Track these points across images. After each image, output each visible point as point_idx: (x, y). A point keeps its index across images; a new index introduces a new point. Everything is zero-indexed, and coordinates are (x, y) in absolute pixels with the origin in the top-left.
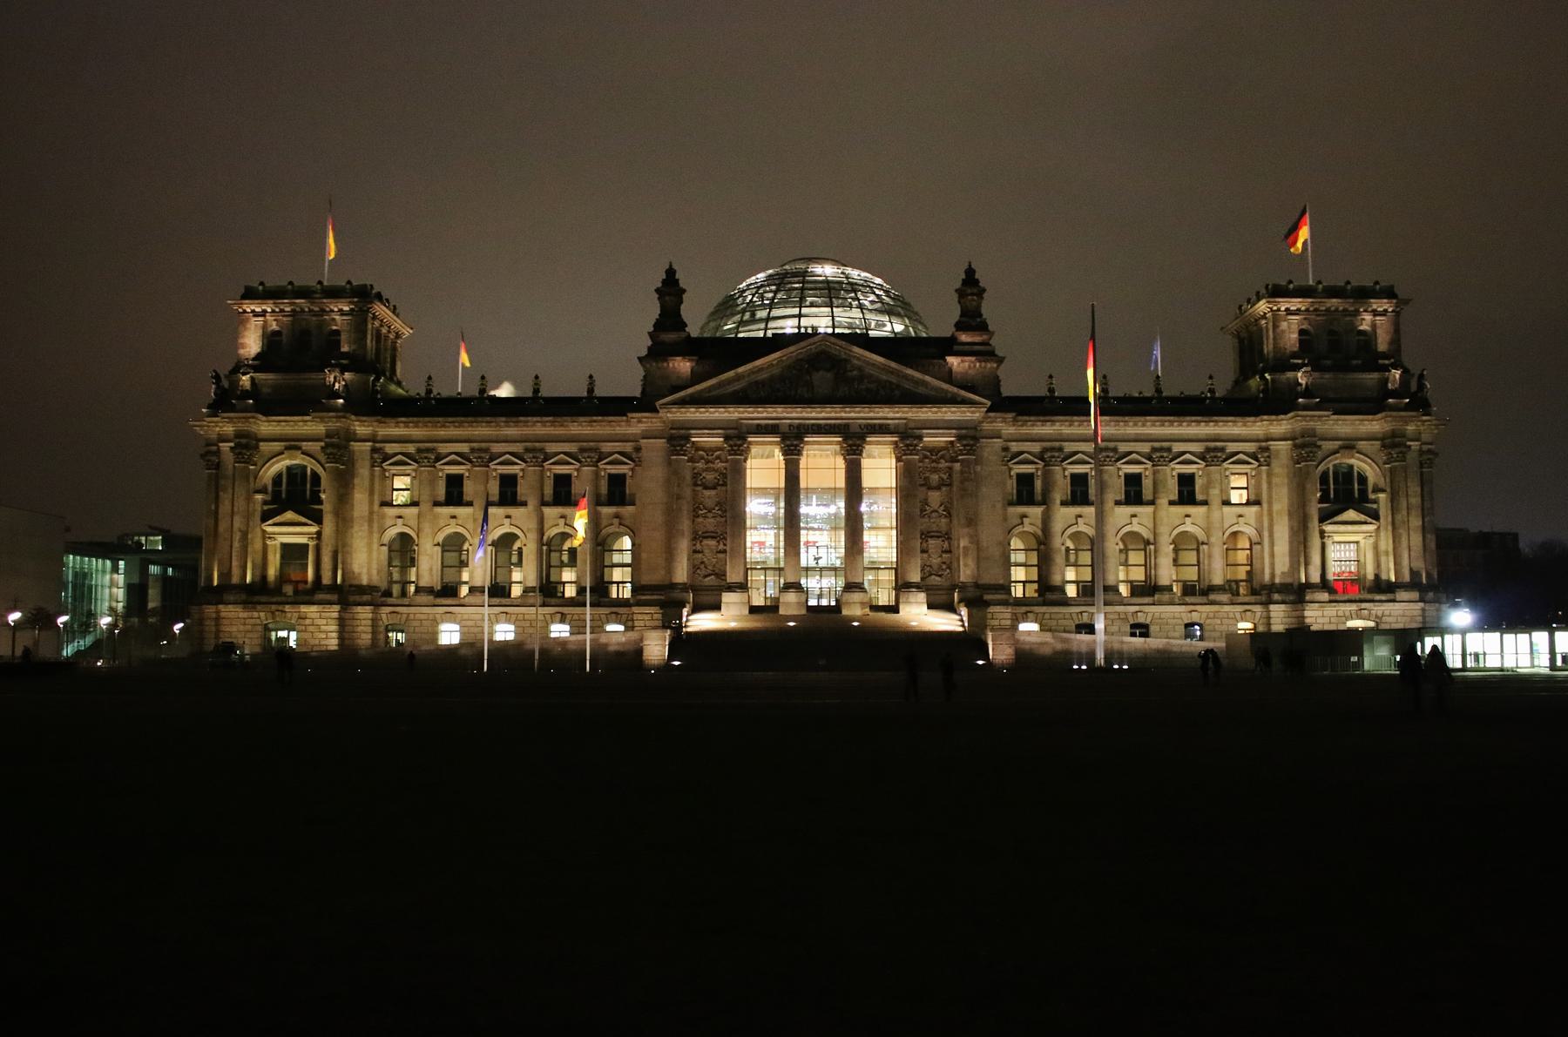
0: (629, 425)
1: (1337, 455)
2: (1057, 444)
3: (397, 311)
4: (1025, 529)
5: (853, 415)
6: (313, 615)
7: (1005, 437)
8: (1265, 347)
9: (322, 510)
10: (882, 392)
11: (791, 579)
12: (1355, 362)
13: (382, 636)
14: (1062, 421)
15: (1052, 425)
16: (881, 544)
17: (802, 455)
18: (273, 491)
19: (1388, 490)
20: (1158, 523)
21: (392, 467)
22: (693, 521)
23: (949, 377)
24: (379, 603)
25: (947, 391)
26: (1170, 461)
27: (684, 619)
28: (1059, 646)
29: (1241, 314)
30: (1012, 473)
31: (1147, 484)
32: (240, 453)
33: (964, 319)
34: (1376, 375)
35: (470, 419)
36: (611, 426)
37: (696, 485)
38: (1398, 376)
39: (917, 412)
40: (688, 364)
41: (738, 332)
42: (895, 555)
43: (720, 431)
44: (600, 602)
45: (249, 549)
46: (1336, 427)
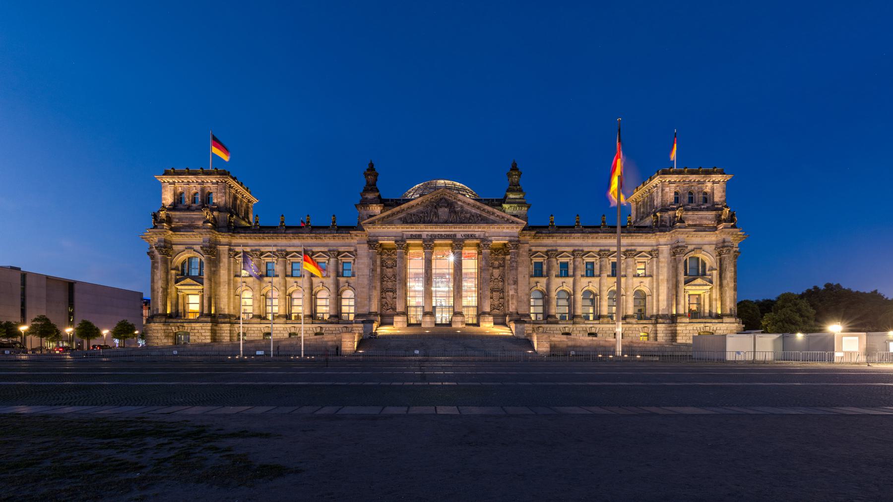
0: (352, 239)
1: (693, 252)
2: (554, 248)
4: (538, 288)
11: (428, 309)
15: (552, 238)
19: (718, 269)
20: (602, 285)
26: (609, 256)
31: (597, 267)
34: (714, 213)
36: (343, 239)
45: (169, 297)
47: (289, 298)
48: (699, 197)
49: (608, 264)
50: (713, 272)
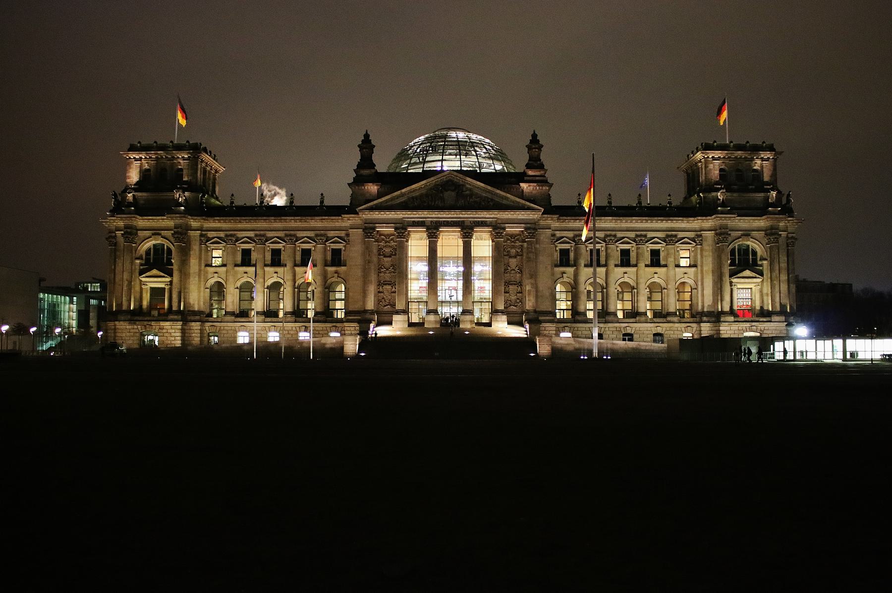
3: (216, 158)
4: (564, 280)
5: (466, 216)
6: (167, 327)
7: (553, 229)
8: (701, 178)
9: (172, 269)
11: (431, 307)
12: (751, 187)
13: (206, 339)
16: (483, 286)
17: (439, 238)
18: (146, 258)
19: (769, 259)
21: (211, 245)
22: (378, 275)
23: (521, 195)
24: (205, 321)
26: (646, 242)
27: (371, 329)
28: (577, 346)
29: (688, 159)
30: (557, 249)
31: (633, 255)
33: (531, 162)
34: (762, 195)
36: (333, 222)
37: (379, 255)
38: (774, 195)
39: (503, 214)
40: (376, 187)
41: (408, 169)
42: (491, 294)
43: (392, 225)
44: (326, 320)
45: (132, 291)
46: (739, 223)
47: (267, 291)
49: (646, 251)
50: (764, 262)
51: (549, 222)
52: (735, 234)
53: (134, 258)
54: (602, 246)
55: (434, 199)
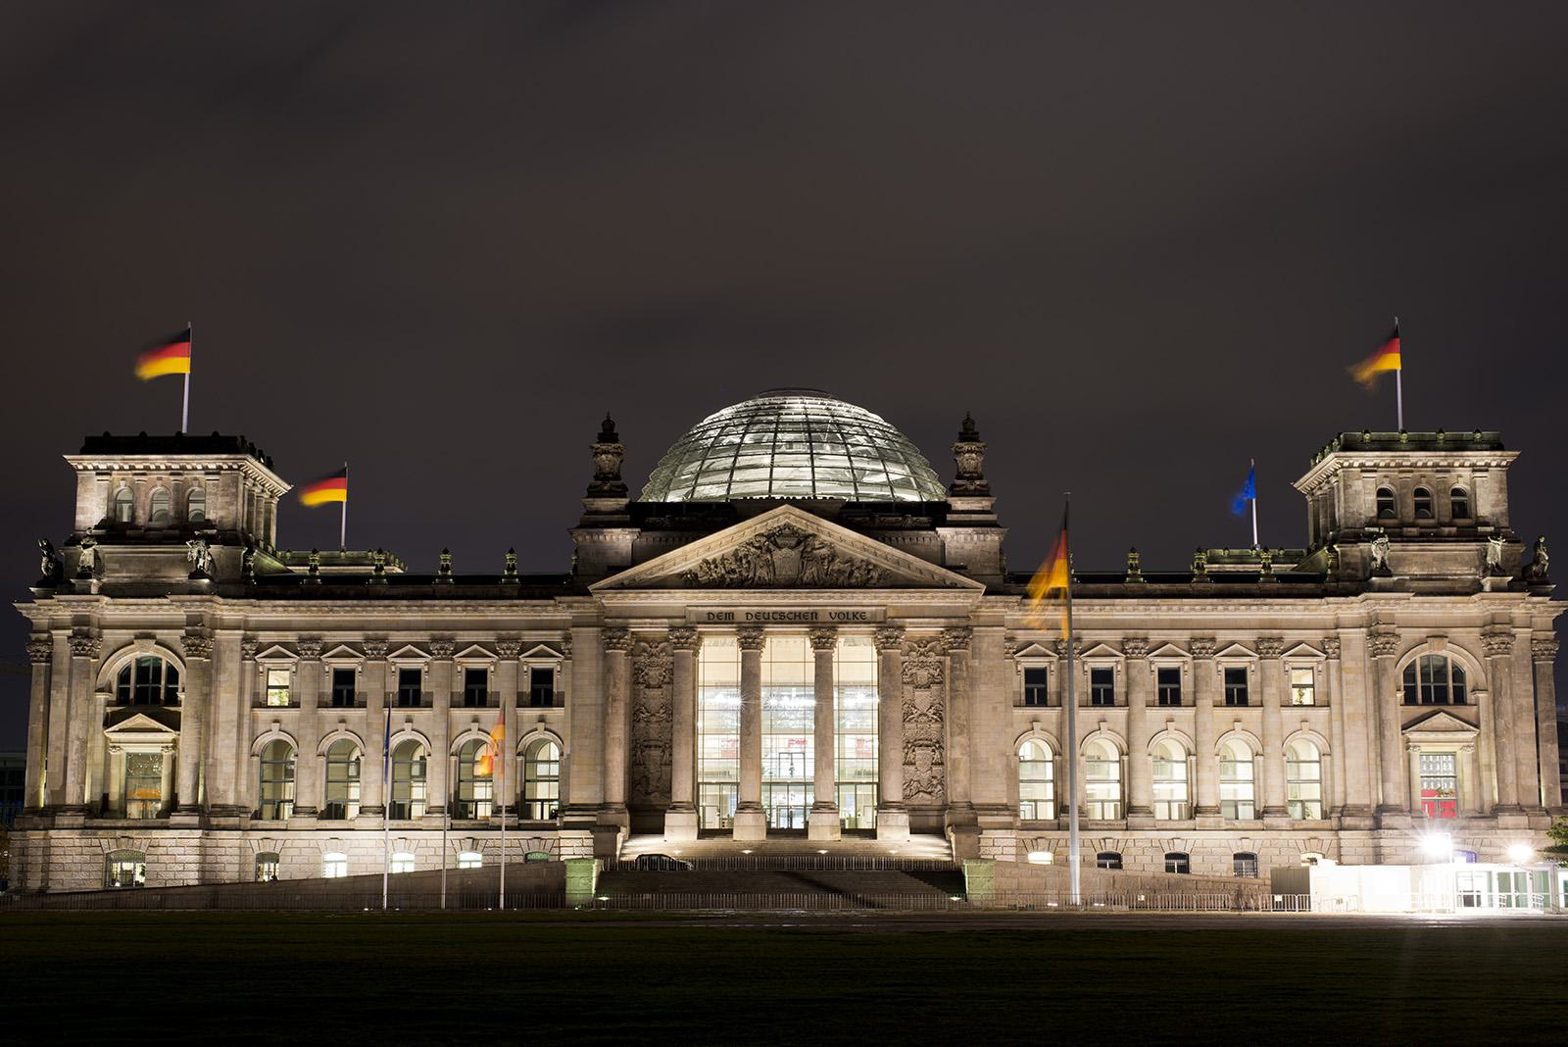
5: (821, 601)
6: (167, 843)
7: (1011, 626)
8: (1336, 510)
10: (856, 574)
12: (1446, 530)
13: (252, 868)
14: (1079, 605)
19: (1490, 689)
20: (1200, 729)
21: (267, 660)
25: (932, 574)
27: (619, 846)
30: (1019, 668)
32: (80, 644)
34: (1473, 546)
35: (365, 602)
38: (1499, 548)
40: (628, 537)
48: (1443, 505)
49: (1214, 671)
51: (999, 610)
52: (1405, 633)
53: (92, 690)
54: (1117, 662)
55: (752, 566)
